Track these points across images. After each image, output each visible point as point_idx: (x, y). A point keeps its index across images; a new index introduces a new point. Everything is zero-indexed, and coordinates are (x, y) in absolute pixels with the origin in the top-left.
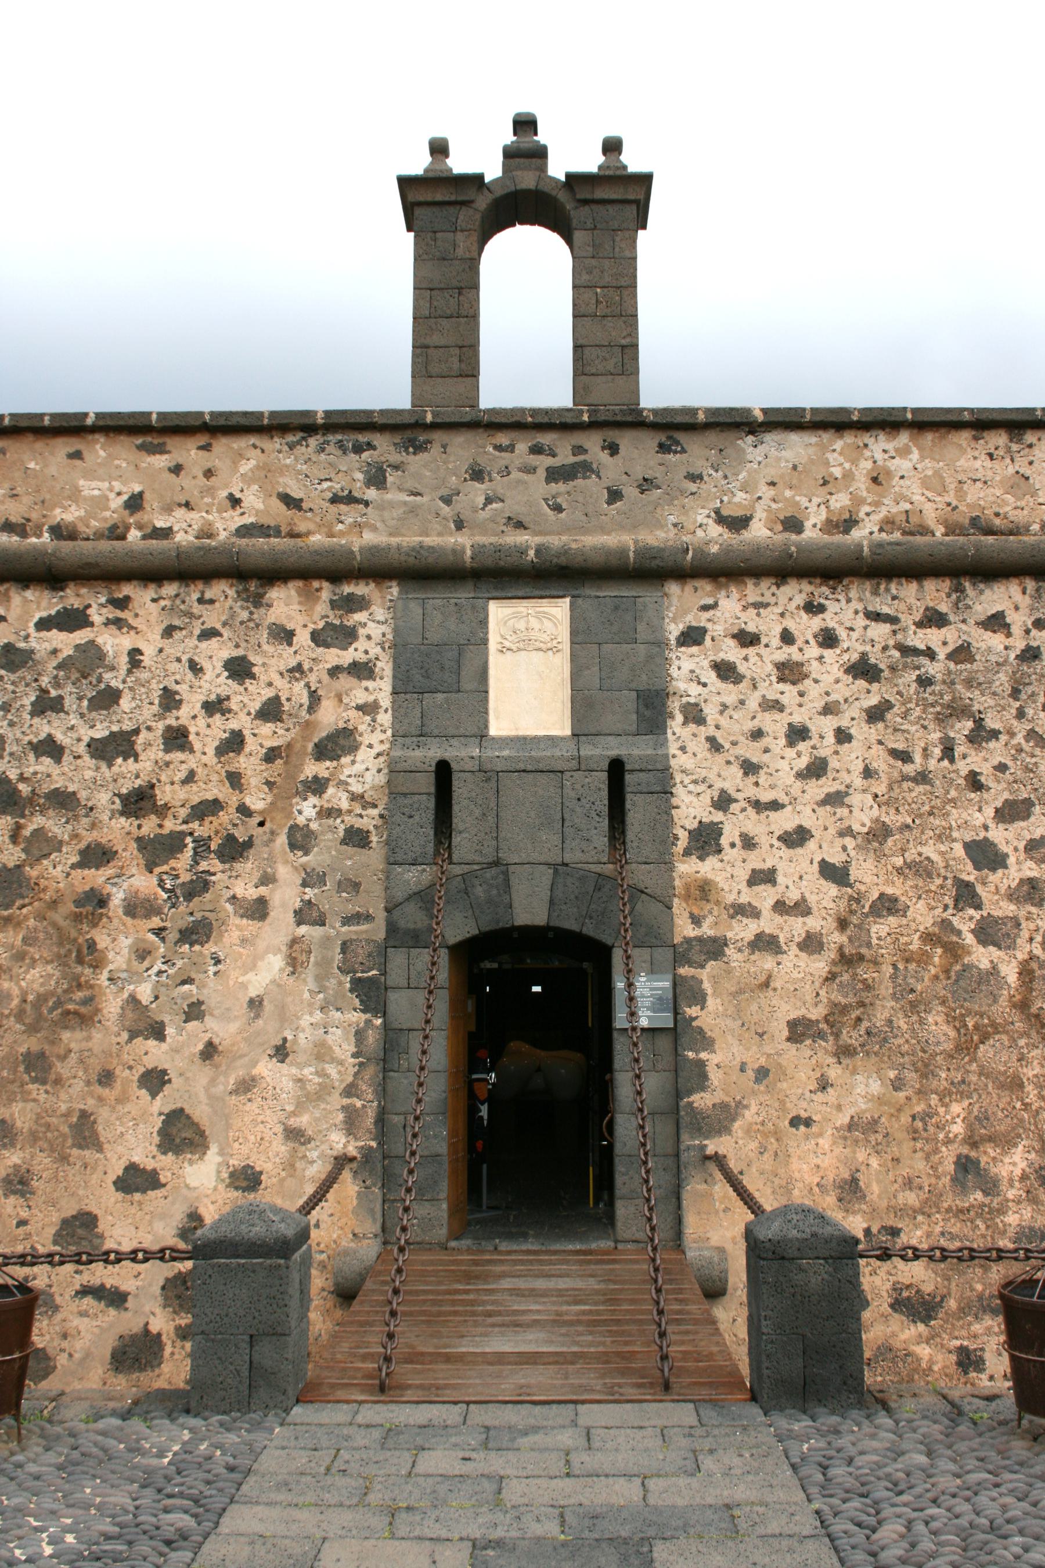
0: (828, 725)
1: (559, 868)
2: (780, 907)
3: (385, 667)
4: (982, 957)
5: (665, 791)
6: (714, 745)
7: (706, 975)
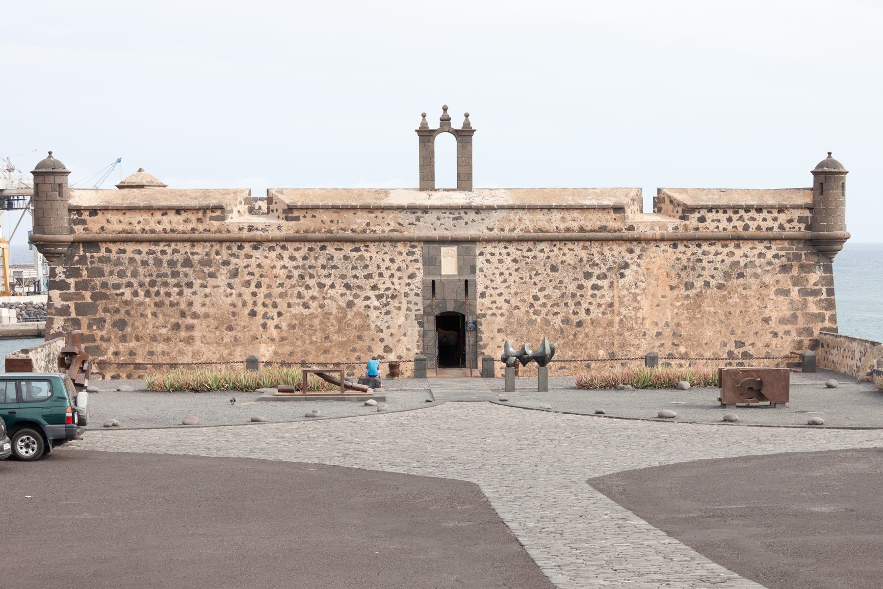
0: (507, 272)
1: (455, 301)
2: (497, 308)
3: (421, 260)
4: (534, 317)
5: (475, 285)
6: (485, 276)
7: (483, 320)
